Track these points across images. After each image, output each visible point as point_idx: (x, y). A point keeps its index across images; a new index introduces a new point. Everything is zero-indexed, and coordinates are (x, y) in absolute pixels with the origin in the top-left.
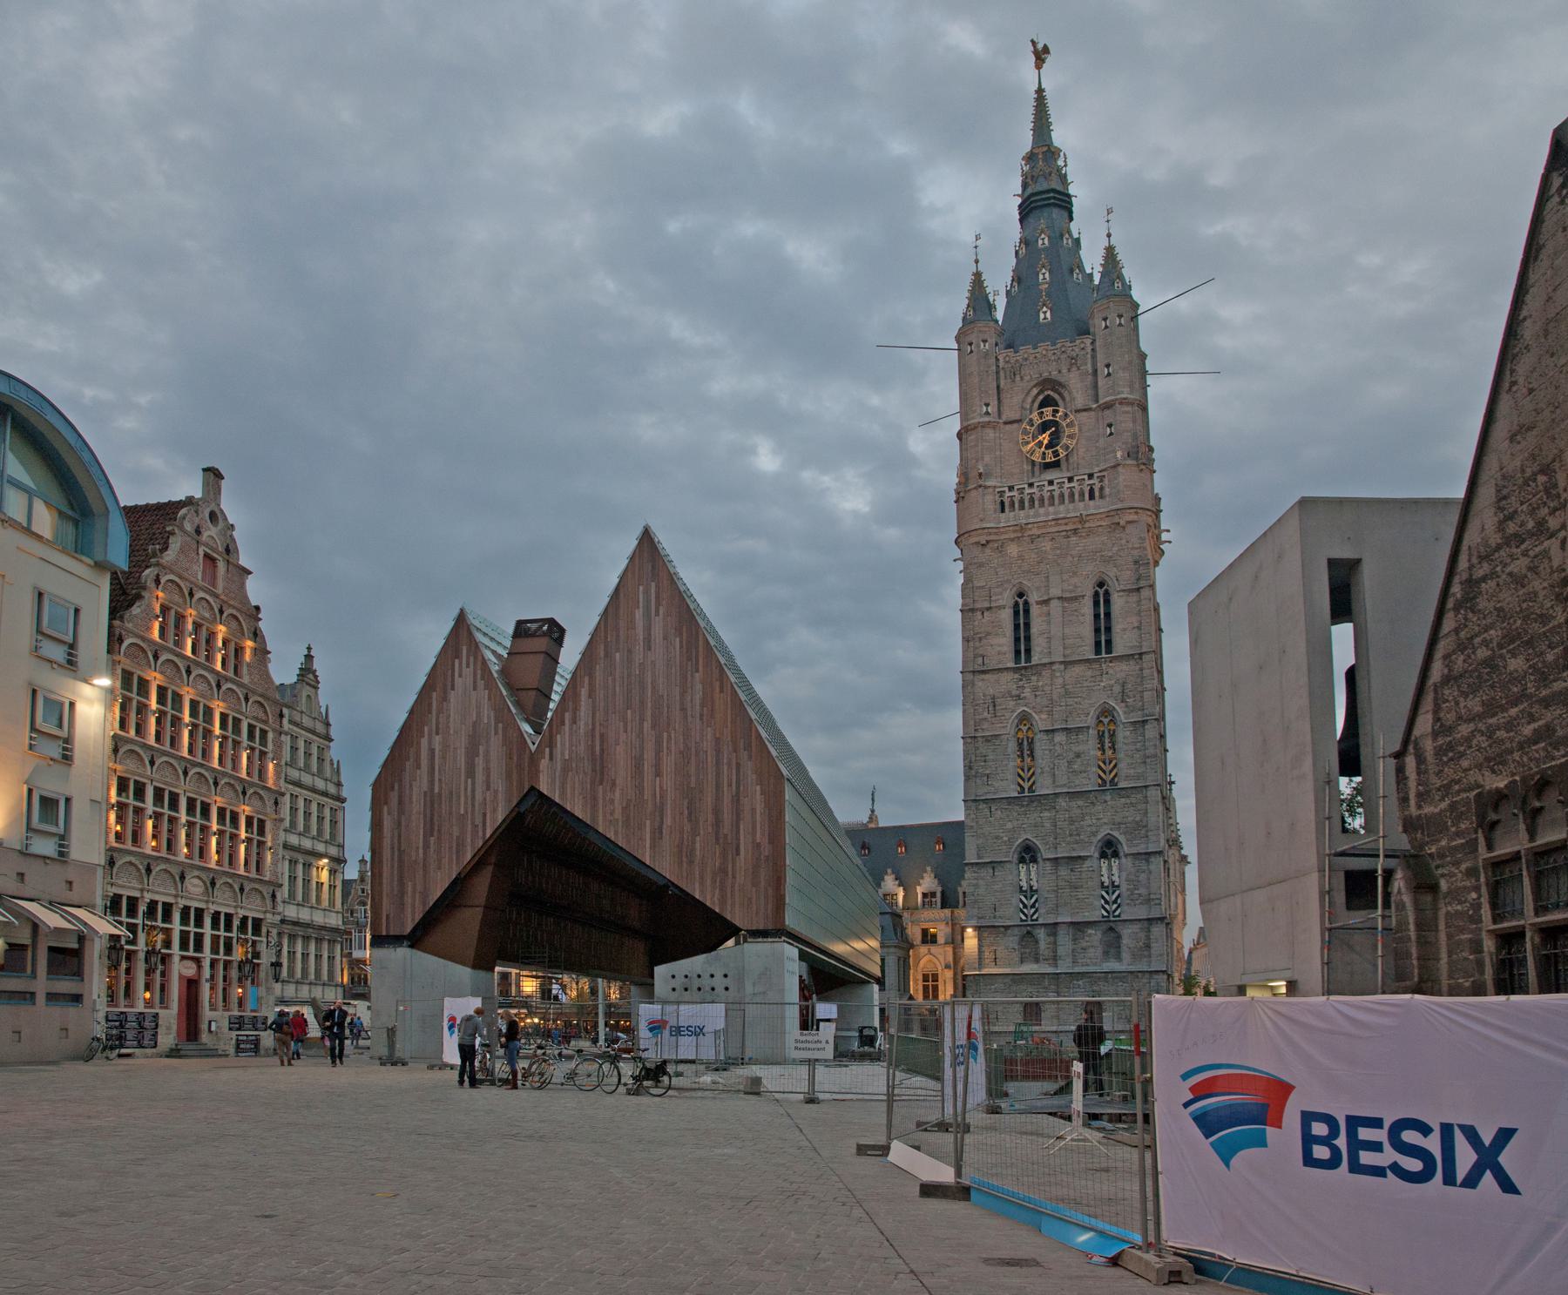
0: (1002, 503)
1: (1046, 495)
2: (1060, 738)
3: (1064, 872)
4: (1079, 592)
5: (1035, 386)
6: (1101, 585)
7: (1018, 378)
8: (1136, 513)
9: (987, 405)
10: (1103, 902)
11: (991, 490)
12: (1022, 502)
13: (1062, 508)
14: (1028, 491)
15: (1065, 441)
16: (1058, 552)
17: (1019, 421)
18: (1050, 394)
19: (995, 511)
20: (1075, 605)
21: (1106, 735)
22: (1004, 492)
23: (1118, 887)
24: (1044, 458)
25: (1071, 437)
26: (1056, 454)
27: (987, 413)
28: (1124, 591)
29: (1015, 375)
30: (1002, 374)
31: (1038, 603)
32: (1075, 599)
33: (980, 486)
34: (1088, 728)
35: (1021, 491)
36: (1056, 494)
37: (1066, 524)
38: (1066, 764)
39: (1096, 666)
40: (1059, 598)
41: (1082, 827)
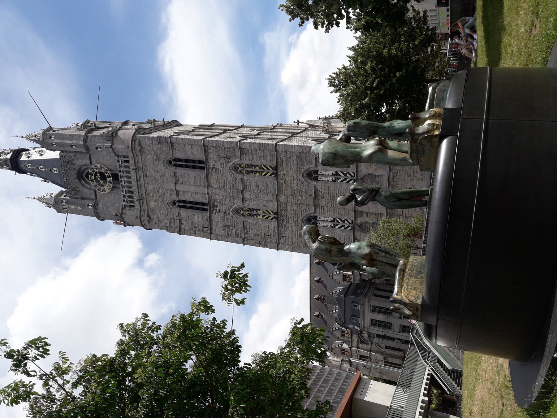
0: (131, 206)
1: (126, 184)
2: (247, 195)
3: (323, 202)
4: (173, 174)
5: (80, 182)
6: (170, 162)
7: (77, 189)
8: (135, 140)
9: (88, 205)
10: (344, 182)
11: (124, 211)
14: (124, 193)
16: (154, 182)
17: (95, 191)
20: (180, 178)
21: (248, 169)
22: (125, 205)
23: (336, 172)
24: (111, 183)
25: (101, 168)
27: (92, 206)
28: (173, 151)
29: (76, 190)
30: (76, 196)
31: (179, 196)
32: (176, 177)
33: (121, 216)
34: (243, 179)
38: (262, 193)
39: (210, 171)
40: (175, 185)
41: (298, 189)
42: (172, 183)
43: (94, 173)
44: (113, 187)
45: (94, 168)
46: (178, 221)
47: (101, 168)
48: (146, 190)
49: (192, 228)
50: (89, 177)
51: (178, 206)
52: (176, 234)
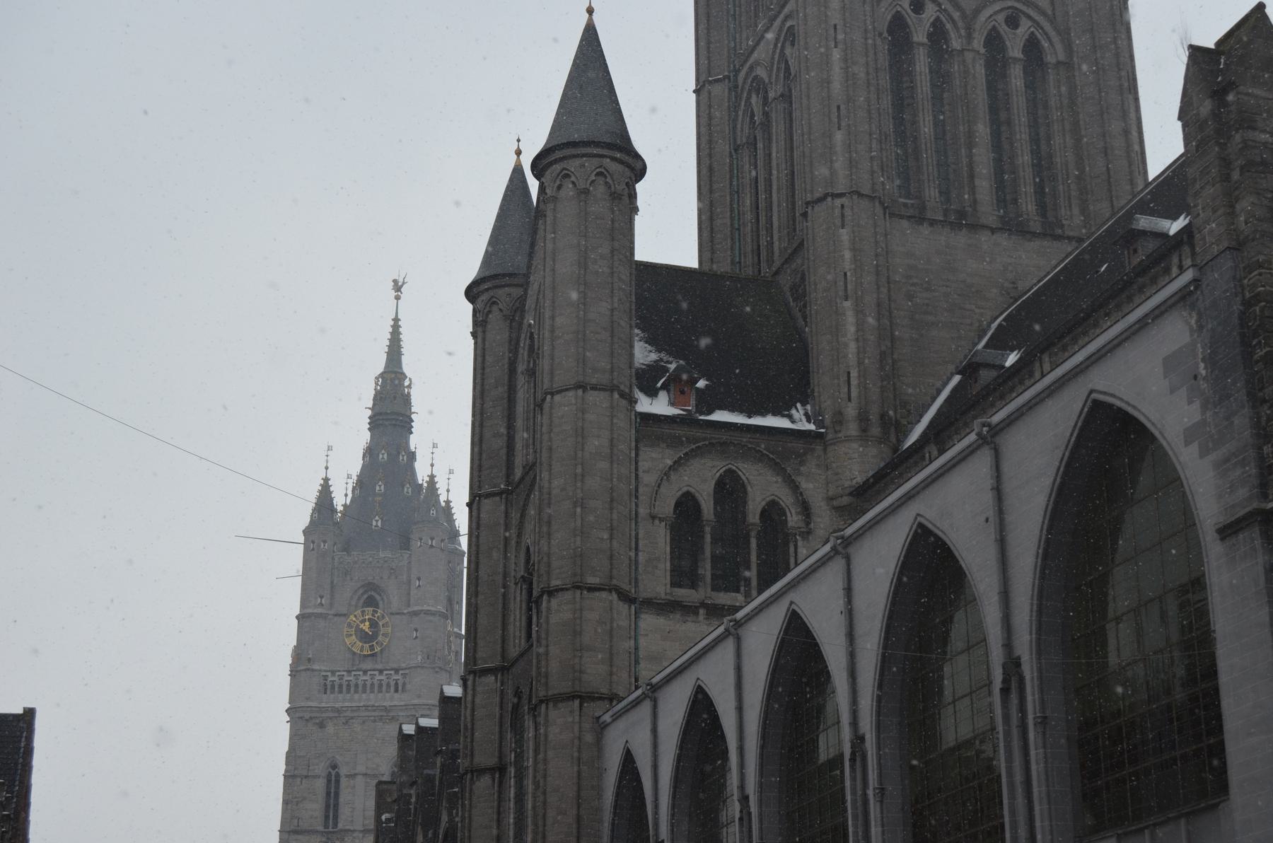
1: (360, 683)
7: (348, 578)
8: (429, 709)
9: (322, 597)
12: (341, 686)
13: (372, 696)
15: (380, 638)
18: (371, 597)
19: (319, 691)
24: (361, 651)
25: (385, 635)
26: (372, 648)
27: (321, 604)
31: (346, 777)
35: (341, 677)
36: (368, 683)
37: (374, 711)
42: (367, 768)
43: (376, 619)
44: (354, 654)
45: (384, 621)
46: (305, 774)
47: (385, 635)
48: (352, 718)
49: (296, 797)
50: (370, 609)
51: (330, 772)
52: (285, 767)
